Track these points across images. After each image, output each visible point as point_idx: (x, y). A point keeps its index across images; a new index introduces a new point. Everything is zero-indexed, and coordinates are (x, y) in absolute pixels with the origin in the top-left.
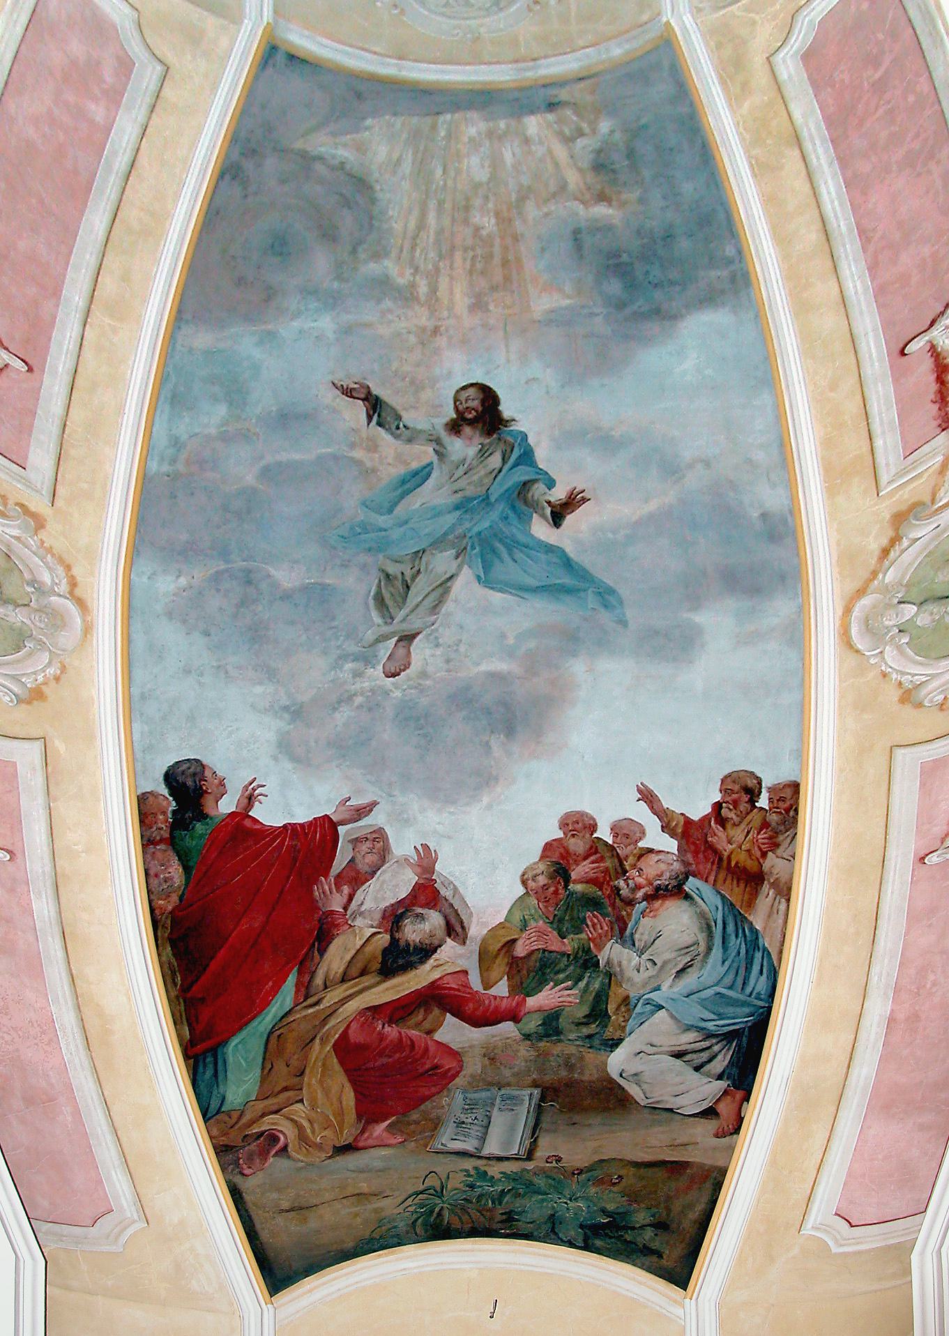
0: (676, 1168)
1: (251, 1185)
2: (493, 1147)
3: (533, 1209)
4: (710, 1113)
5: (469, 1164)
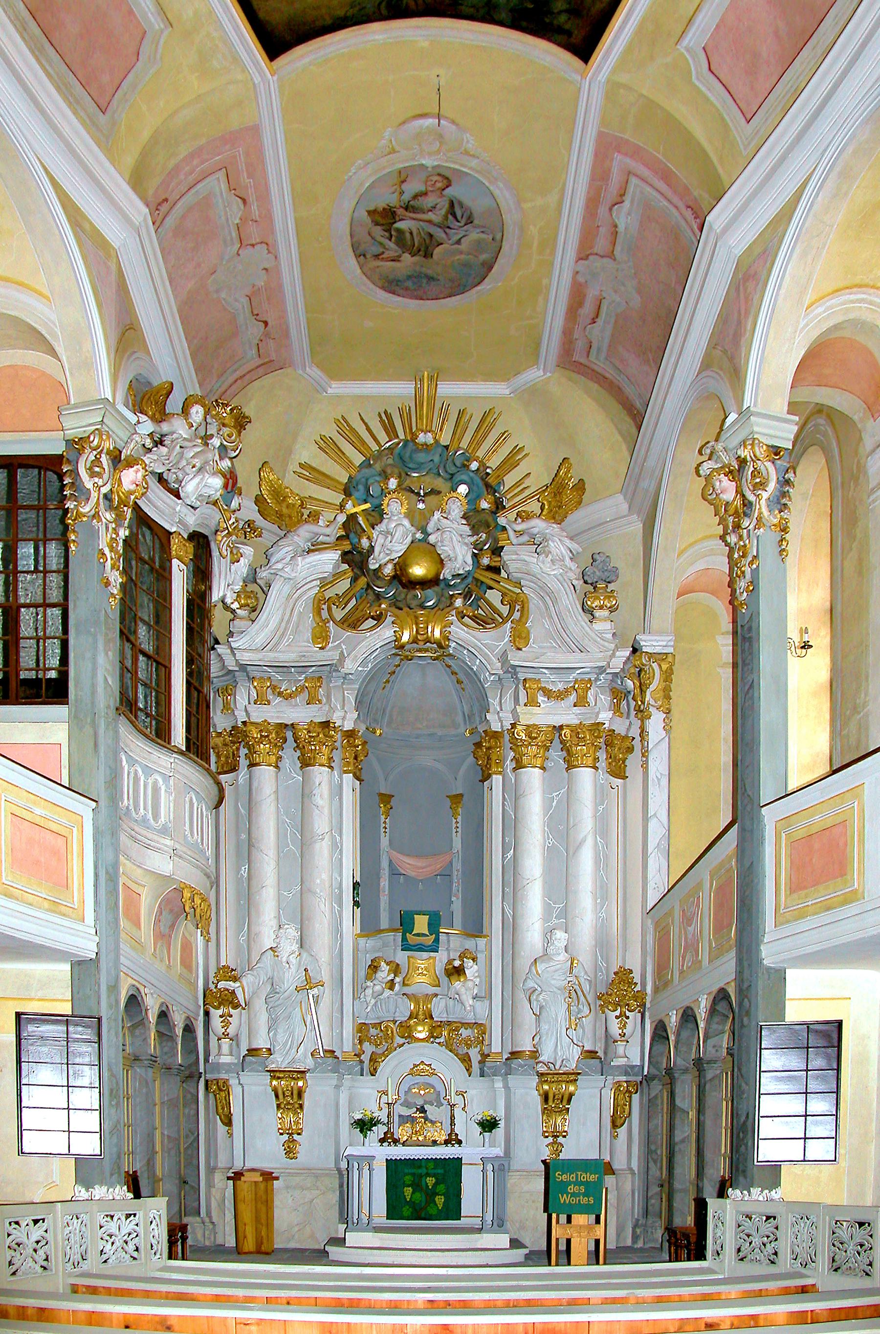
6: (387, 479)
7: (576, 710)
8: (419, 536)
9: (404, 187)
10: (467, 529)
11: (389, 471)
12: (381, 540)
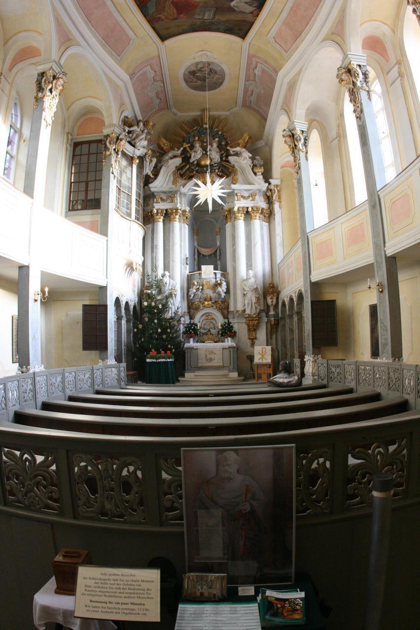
0: (245, 21)
1: (157, 26)
2: (206, 17)
3: (214, 27)
4: (252, 13)
5: (201, 20)
6: (195, 137)
7: (253, 202)
8: (204, 152)
9: (198, 66)
10: (218, 150)
11: (195, 135)
12: (193, 154)
